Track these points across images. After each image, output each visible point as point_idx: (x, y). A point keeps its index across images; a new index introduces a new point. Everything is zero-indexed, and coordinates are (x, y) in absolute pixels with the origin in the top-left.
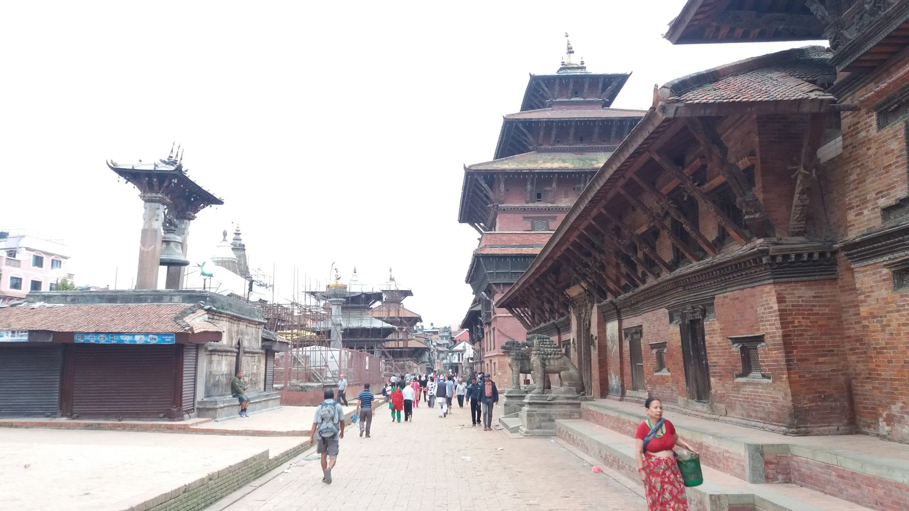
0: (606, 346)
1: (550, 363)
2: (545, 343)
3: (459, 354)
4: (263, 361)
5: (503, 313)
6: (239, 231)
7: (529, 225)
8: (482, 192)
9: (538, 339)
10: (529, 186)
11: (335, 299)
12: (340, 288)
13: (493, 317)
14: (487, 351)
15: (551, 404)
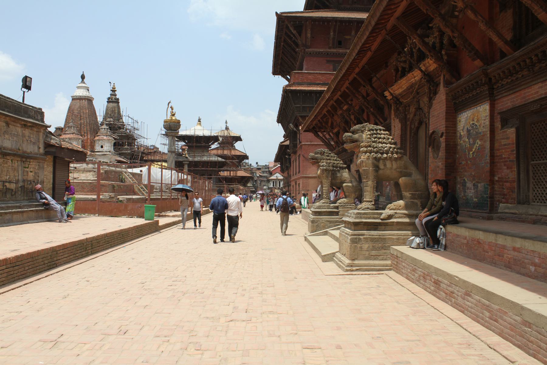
0: (455, 145)
1: (385, 165)
2: (379, 136)
3: (273, 182)
4: (51, 169)
5: (307, 142)
6: (115, 88)
7: (332, 67)
8: (291, 38)
9: (369, 131)
10: (332, 34)
11: (170, 131)
12: (174, 122)
13: (298, 146)
14: (293, 175)
15: (386, 225)
